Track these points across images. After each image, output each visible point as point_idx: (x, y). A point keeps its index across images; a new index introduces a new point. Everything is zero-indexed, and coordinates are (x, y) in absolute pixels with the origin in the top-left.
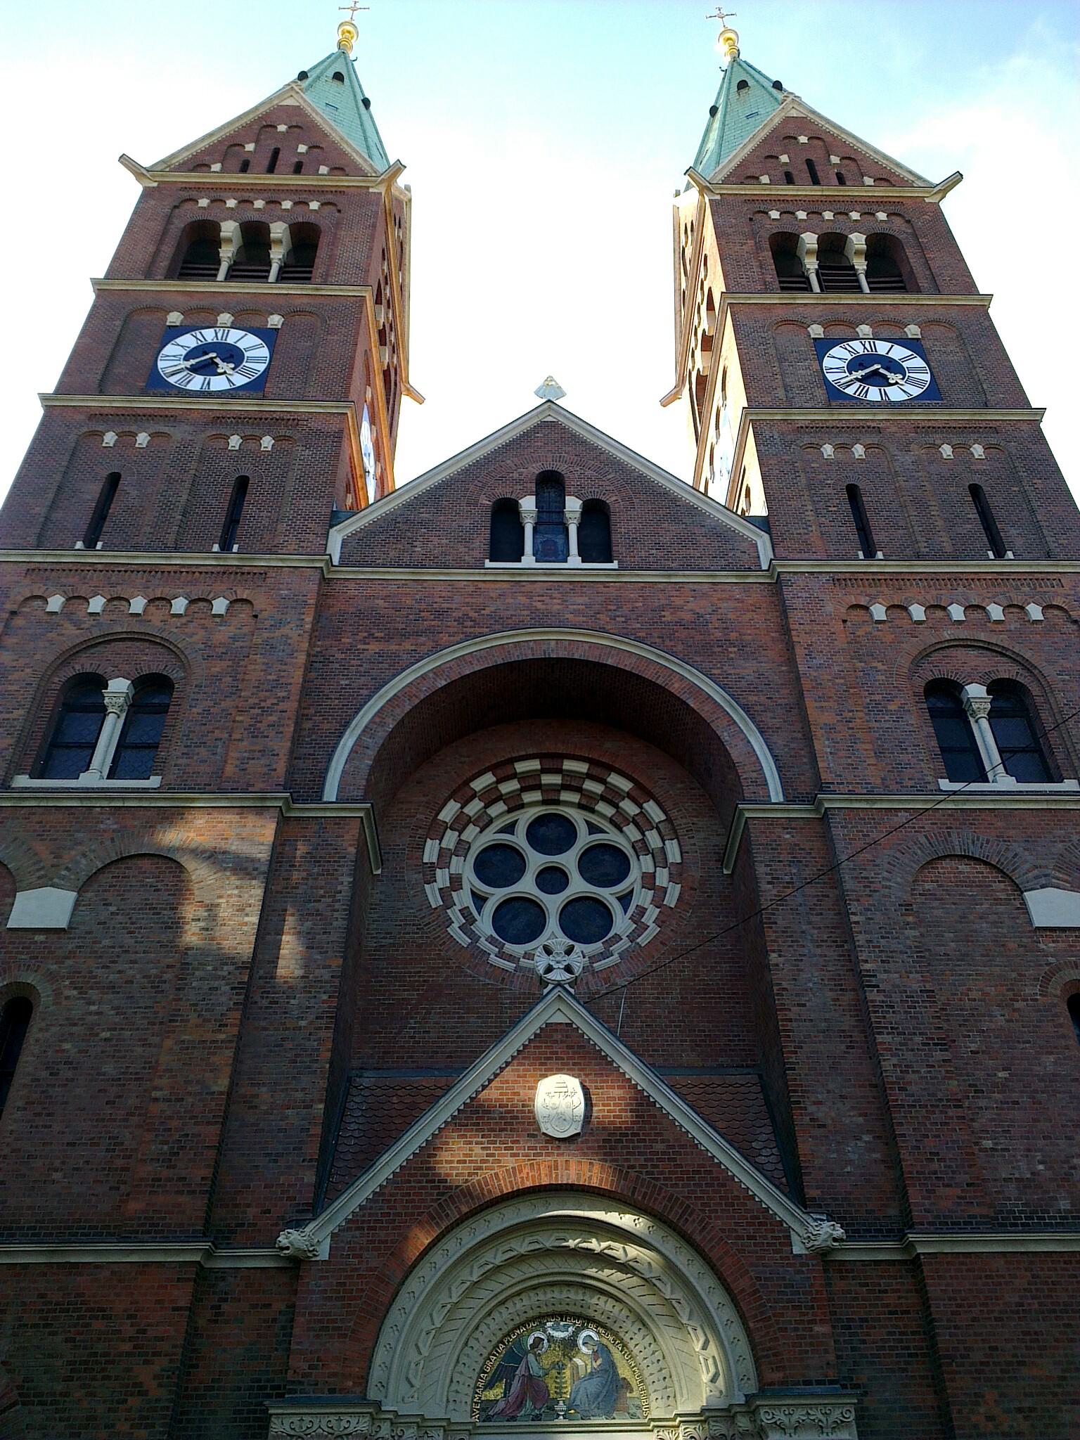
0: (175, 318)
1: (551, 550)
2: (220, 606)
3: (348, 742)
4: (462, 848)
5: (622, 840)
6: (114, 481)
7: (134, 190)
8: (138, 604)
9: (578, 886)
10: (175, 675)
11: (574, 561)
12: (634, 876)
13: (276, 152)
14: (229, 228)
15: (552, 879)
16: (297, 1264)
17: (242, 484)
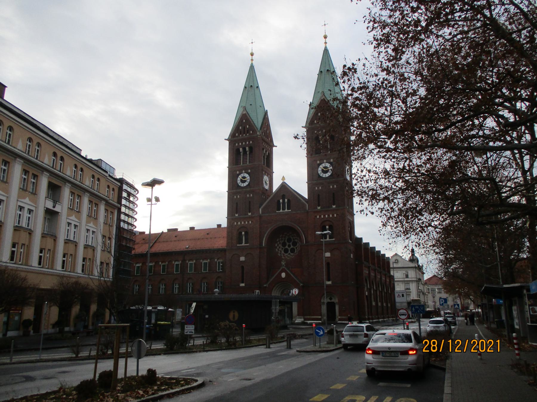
0: (238, 172)
1: (284, 209)
3: (264, 239)
4: (280, 243)
5: (296, 241)
6: (237, 203)
7: (227, 142)
8: (243, 223)
9: (292, 247)
11: (286, 210)
12: (297, 246)
13: (244, 127)
14: (241, 149)
15: (289, 246)
16: (266, 287)
17: (250, 202)
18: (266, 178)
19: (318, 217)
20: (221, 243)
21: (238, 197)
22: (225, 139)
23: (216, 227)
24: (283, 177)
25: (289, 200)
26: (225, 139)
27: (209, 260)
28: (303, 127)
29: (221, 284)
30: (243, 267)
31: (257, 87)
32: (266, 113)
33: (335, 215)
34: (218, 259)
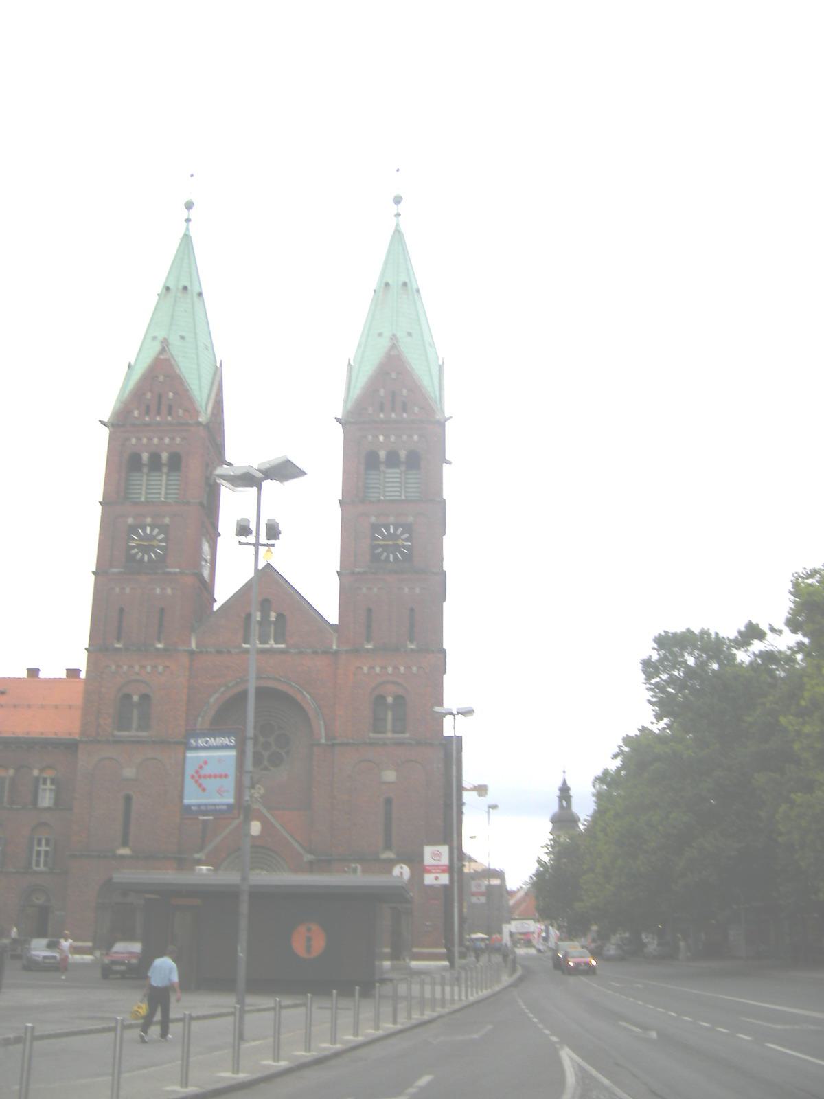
2: (160, 669)
7: (106, 432)
13: (160, 397)
18: (206, 548)
19: (365, 669)
20: (66, 725)
21: (128, 591)
22: (103, 423)
23: (24, 675)
25: (280, 616)
26: (103, 423)
27: (11, 772)
29: (47, 844)
30: (128, 799)
31: (200, 294)
32: (217, 372)
33: (415, 669)
34: (42, 770)
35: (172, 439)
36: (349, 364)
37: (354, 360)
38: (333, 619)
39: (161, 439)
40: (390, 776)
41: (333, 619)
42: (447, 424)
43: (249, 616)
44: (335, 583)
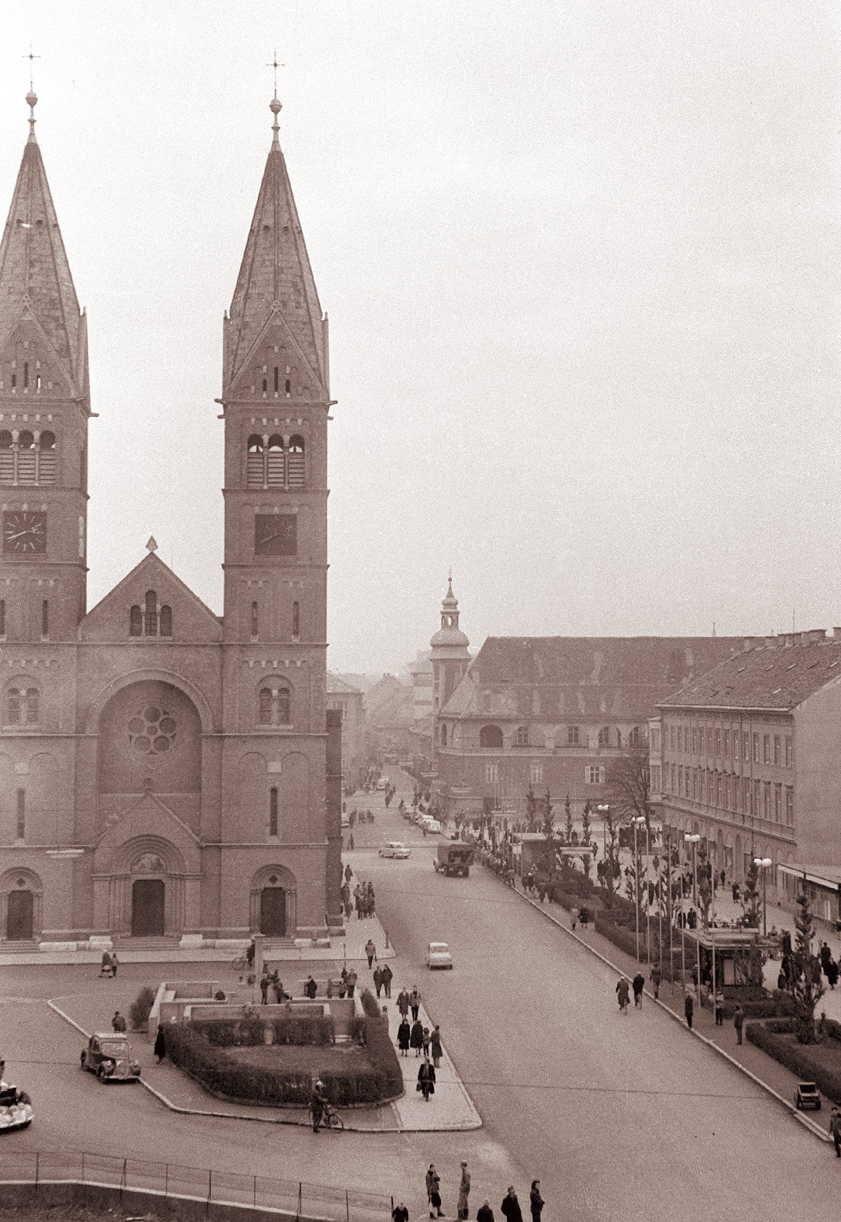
10: (39, 689)
24: (152, 539)
25: (166, 609)
28: (217, 401)
35: (43, 416)
36: (225, 318)
37: (230, 312)
38: (219, 612)
39: (32, 415)
40: (275, 767)
41: (219, 612)
42: (331, 407)
43: (135, 608)
44: (220, 575)
